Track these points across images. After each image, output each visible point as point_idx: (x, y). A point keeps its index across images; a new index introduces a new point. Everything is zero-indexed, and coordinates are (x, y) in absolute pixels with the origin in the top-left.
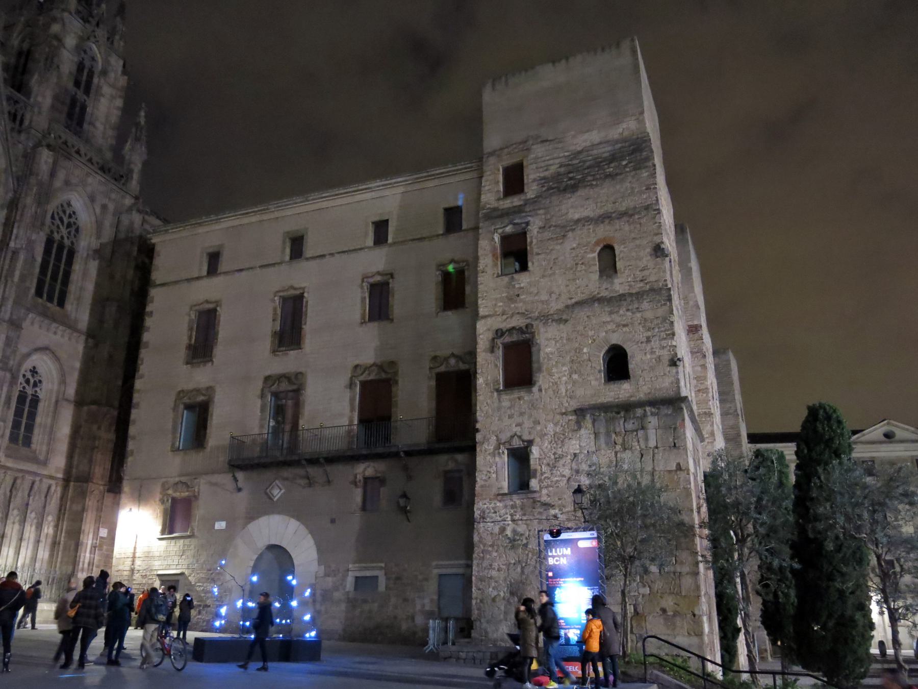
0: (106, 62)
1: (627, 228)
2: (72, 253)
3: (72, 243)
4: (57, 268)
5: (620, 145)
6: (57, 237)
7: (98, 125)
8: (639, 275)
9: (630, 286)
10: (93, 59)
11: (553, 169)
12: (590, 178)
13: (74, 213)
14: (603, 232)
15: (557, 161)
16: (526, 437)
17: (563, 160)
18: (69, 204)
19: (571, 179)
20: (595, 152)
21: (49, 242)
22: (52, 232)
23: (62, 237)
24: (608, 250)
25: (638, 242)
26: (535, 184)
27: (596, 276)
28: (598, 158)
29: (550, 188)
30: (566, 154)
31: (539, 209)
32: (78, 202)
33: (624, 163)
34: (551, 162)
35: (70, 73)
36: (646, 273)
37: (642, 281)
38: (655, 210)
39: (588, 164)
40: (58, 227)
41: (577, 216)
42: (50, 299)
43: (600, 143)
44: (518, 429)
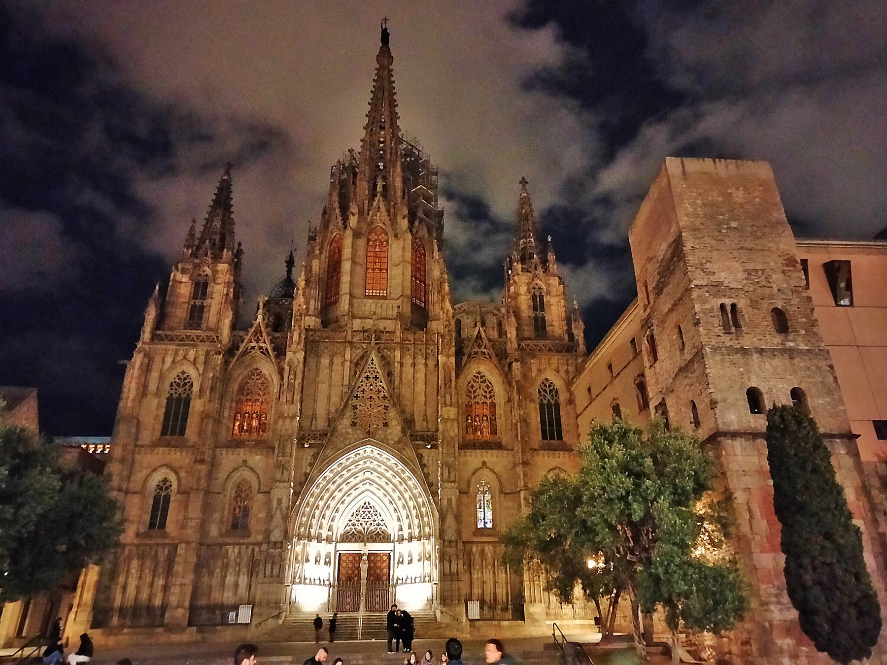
0: (548, 285)
2: (557, 405)
3: (556, 400)
4: (550, 418)
6: (545, 402)
7: (555, 323)
10: (540, 288)
13: (552, 383)
18: (547, 380)
19: (661, 282)
21: (542, 406)
22: (542, 400)
23: (549, 400)
32: (551, 376)
35: (529, 306)
40: (545, 396)
42: (552, 438)
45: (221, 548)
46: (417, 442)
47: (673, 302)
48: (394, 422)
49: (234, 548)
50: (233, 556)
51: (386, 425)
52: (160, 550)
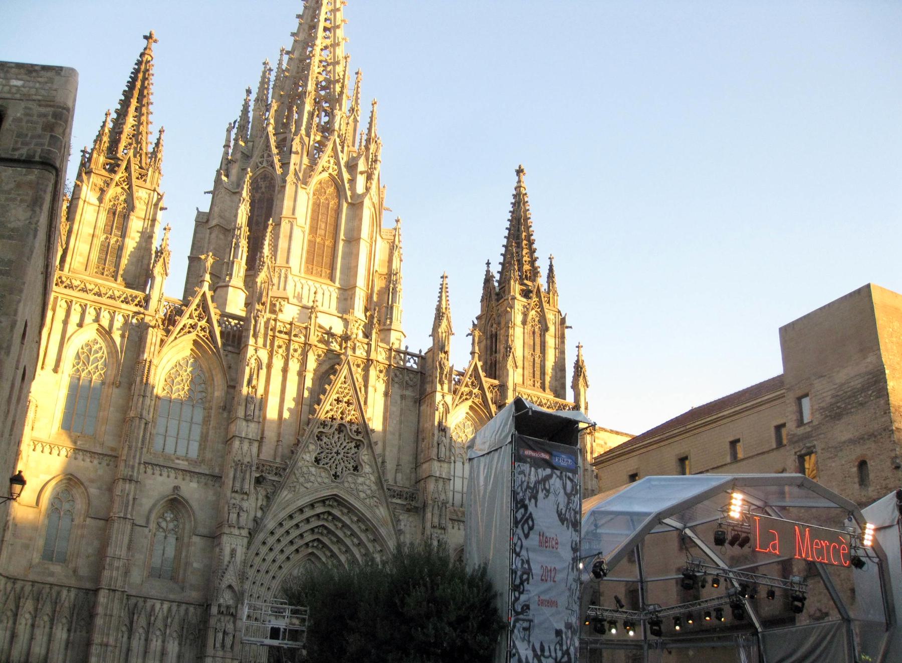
1: (873, 446)
5: (867, 377)
8: (884, 483)
9: (878, 492)
11: (828, 399)
12: (849, 407)
14: (857, 452)
15: (830, 393)
16: (824, 611)
17: (833, 392)
19: (839, 407)
20: (852, 384)
24: (862, 465)
25: (881, 457)
26: (817, 413)
27: (857, 486)
28: (854, 389)
29: (827, 416)
30: (835, 386)
31: (820, 434)
33: (870, 392)
34: (824, 395)
36: (887, 481)
37: (885, 488)
38: (890, 431)
39: (848, 394)
41: (843, 439)
43: (856, 376)
44: (818, 605)
45: (145, 602)
46: (394, 500)
47: (857, 434)
48: (367, 469)
49: (162, 604)
50: (160, 614)
51: (356, 468)
52: (64, 593)
